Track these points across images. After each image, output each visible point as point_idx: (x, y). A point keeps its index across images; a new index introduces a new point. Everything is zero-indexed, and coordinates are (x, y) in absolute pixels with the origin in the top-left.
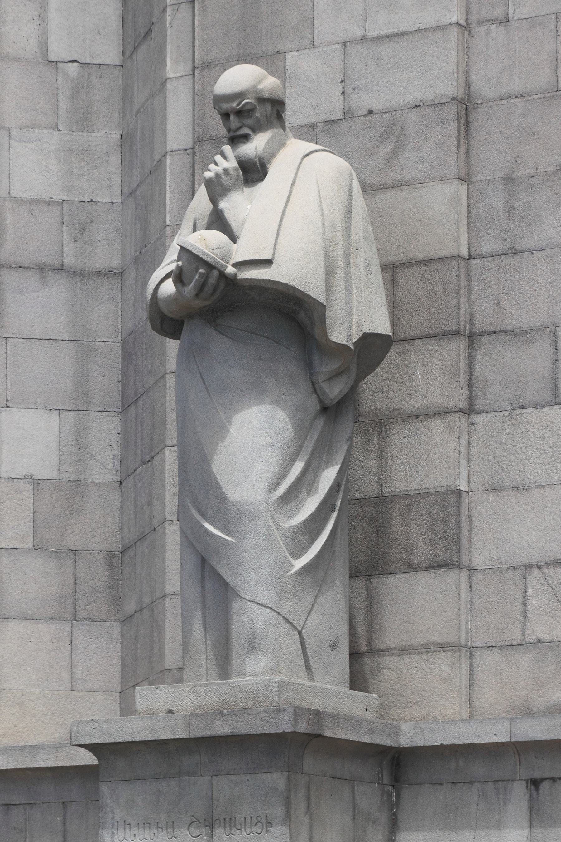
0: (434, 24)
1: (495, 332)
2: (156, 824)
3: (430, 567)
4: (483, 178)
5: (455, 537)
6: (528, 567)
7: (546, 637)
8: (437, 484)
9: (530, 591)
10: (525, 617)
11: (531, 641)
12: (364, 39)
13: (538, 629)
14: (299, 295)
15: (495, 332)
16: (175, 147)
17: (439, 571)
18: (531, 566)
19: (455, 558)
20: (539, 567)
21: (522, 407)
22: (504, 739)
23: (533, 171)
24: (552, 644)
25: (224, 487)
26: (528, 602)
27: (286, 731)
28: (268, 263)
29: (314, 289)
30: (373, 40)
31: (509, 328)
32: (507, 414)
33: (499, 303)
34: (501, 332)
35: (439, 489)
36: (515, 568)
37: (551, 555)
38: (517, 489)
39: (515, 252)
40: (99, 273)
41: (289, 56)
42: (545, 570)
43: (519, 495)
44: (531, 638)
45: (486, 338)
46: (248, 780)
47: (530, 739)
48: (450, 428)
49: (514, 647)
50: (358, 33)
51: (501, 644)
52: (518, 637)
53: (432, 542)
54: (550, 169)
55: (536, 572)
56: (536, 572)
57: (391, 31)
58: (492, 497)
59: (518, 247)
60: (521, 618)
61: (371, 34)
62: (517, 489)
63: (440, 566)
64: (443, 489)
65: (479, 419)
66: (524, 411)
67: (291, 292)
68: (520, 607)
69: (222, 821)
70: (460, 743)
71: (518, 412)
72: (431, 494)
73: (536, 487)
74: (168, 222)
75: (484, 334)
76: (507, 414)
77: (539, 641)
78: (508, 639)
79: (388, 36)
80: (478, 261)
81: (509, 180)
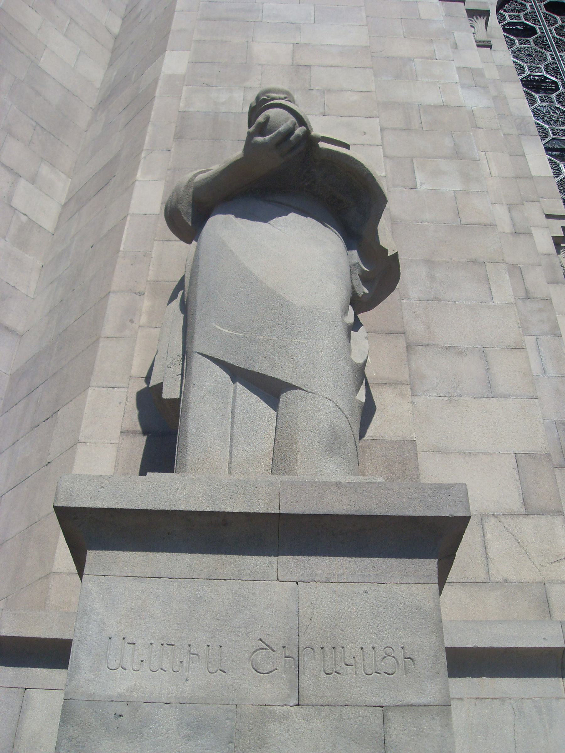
1: (428, 345)
2: (186, 646)
4: (405, 257)
5: (415, 477)
7: (513, 578)
8: (392, 434)
9: (489, 536)
10: (487, 558)
11: (498, 580)
13: (503, 569)
15: (428, 345)
18: (488, 515)
21: (460, 396)
23: (449, 260)
24: (520, 584)
26: (489, 546)
31: (441, 343)
33: (429, 328)
35: (395, 439)
38: (463, 453)
42: (503, 519)
45: (421, 347)
49: (479, 584)
51: (462, 580)
52: (482, 576)
55: (493, 520)
60: (483, 559)
62: (463, 453)
64: (398, 439)
65: (416, 399)
70: (500, 646)
71: (456, 399)
72: (386, 441)
73: (485, 454)
74: (121, 249)
76: (446, 399)
77: (506, 581)
78: (471, 577)
80: (408, 302)
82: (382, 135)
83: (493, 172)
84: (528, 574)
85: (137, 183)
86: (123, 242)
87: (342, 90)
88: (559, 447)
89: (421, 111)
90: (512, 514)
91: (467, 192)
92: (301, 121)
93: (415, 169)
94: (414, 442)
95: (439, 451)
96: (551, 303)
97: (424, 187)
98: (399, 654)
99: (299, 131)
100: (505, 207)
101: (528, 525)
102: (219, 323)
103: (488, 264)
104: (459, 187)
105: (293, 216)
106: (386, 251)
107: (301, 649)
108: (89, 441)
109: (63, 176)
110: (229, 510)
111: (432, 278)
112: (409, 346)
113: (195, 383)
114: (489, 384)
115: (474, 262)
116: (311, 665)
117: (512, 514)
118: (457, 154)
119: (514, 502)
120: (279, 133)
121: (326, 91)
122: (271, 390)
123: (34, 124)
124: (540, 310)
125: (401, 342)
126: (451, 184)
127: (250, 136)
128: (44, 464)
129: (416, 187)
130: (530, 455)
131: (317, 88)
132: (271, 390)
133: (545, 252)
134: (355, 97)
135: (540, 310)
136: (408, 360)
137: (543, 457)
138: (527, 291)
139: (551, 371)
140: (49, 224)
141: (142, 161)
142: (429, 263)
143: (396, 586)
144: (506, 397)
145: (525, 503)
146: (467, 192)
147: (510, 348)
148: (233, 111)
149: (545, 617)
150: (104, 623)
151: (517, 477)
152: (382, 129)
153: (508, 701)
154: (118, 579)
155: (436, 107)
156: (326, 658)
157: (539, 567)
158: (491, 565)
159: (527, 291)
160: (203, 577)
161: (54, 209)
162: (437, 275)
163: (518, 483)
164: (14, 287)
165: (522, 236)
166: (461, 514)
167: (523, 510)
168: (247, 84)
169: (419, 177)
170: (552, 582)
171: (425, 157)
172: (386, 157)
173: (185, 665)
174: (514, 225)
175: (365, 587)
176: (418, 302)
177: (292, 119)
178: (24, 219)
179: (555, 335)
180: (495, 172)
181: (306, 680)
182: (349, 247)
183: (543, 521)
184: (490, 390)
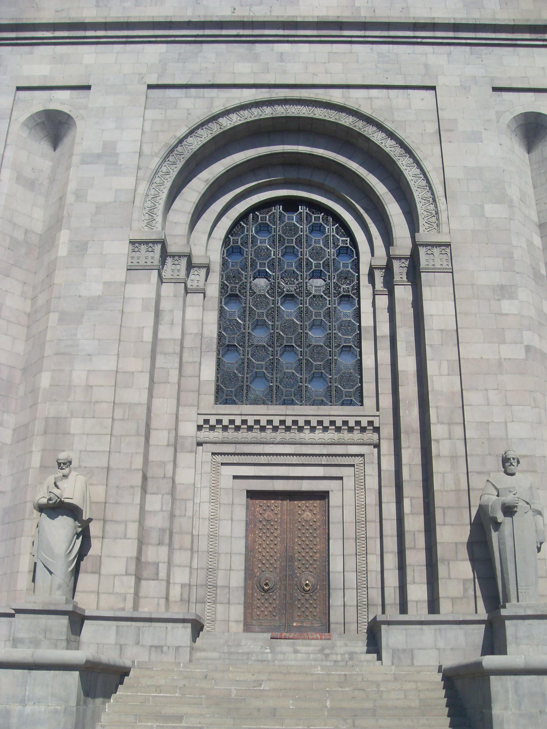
6: (115, 575)
7: (119, 592)
12: (86, 450)
13: (117, 590)
29: (80, 506)
39: (117, 503)
44: (115, 592)
50: (84, 449)
55: (117, 577)
56: (117, 577)
61: (87, 450)
75: (108, 521)
81: (117, 487)
87: (102, 402)
90: (122, 575)
92: (59, 498)
100: (168, 431)
101: (125, 578)
105: (60, 516)
109: (12, 415)
114: (125, 534)
117: (122, 575)
119: (124, 572)
121: (96, 402)
122: (51, 573)
125: (102, 522)
129: (120, 452)
131: (93, 401)
132: (51, 573)
139: (164, 509)
140: (9, 442)
144: (129, 539)
145: (126, 572)
146: (137, 453)
161: (10, 432)
168: (69, 399)
174: (168, 441)
177: (57, 498)
182: (75, 520)
183: (129, 577)
184: (125, 538)
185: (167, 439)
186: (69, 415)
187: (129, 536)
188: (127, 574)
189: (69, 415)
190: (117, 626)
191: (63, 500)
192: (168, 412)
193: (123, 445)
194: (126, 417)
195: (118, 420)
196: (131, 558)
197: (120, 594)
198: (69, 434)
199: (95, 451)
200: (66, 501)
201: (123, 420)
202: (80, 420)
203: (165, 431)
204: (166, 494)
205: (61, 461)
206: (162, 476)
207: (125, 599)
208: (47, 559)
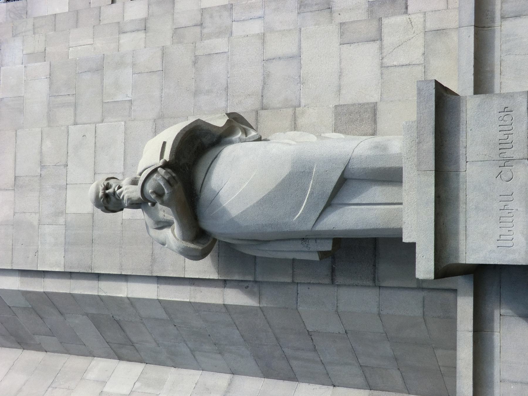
0: (123, 134)
3: (375, 122)
5: (360, 106)
6: (382, 66)
7: (422, 50)
14: (187, 129)
16: (156, 294)
17: (378, 116)
18: (382, 63)
19: (372, 105)
20: (383, 58)
22: (472, 29)
25: (283, 177)
26: (401, 64)
27: (434, 86)
28: (164, 143)
30: (124, 169)
31: (261, 88)
32: (302, 86)
34: (262, 93)
36: (382, 74)
37: (377, 51)
40: (229, 385)
41: (124, 218)
42: (384, 54)
43: (343, 74)
45: (264, 101)
46: (471, 130)
47: (474, 12)
48: (303, 113)
52: (421, 68)
53: (362, 120)
54: (194, 71)
55: (385, 60)
57: (123, 159)
58: (343, 92)
59: (225, 86)
61: (122, 170)
63: (375, 115)
65: (303, 104)
66: (301, 75)
67: (184, 132)
68: (404, 69)
69: (501, 151)
71: (302, 79)
74: (188, 300)
76: (302, 86)
79: (124, 160)
82: (81, 124)
83: (89, 43)
84: (420, 41)
85: (129, 296)
86: (182, 300)
88: (317, 12)
89: (57, 95)
90: (381, 48)
91: (134, 65)
93: (113, 100)
94: (336, 107)
95: (339, 90)
96: (205, 8)
97: (130, 95)
98: (503, 114)
99: (162, 171)
100: (122, 36)
101: (387, 40)
102: (294, 216)
103: (197, 54)
104: (129, 70)
106: (228, 120)
107: (501, 159)
108: (336, 305)
110: (433, 195)
111: (209, 92)
112: (263, 109)
113: (332, 227)
114: (292, 57)
115: (195, 63)
116: (508, 154)
117: (381, 48)
118: (99, 69)
120: (164, 185)
123: (50, 389)
124: (211, 17)
125: (262, 113)
126: (127, 75)
127: (163, 203)
128: (345, 336)
129: (130, 101)
130: (341, 35)
131: (39, 171)
133: (147, 7)
134: (48, 144)
135: (211, 17)
136: (274, 109)
137: (342, 27)
138: (196, 25)
139: (260, 13)
141: (109, 294)
142: (196, 93)
143: (468, 116)
144: (300, 48)
145: (374, 41)
146: (134, 65)
147: (264, 43)
148: (64, 231)
149: (446, 33)
150: (491, 250)
151: (356, 44)
152: (75, 124)
153: (502, 58)
154: (467, 247)
155: (51, 84)
156: (505, 147)
157: (414, 35)
158: (414, 63)
159: (196, 25)
160: (465, 207)
161: (124, 367)
162: (206, 88)
163: (360, 44)
164: (196, 384)
165: (148, 25)
166: (434, 84)
167: (378, 42)
168: (36, 223)
169: (120, 98)
170: (425, 27)
171: (102, 93)
172: (102, 121)
173: (510, 211)
174: (138, 30)
175: (469, 130)
176: (228, 101)
178: (138, 385)
179: (232, 8)
180: (90, 41)
181: (516, 156)
183: (385, 30)
184: (297, 57)
185: (134, 34)
186: (62, 220)
187: (293, 50)
188: (379, 38)
189: (62, 220)
190: (503, 18)
191: (160, 163)
192: (90, 41)
193: (119, 98)
194: (71, 99)
195: (75, 115)
196: (342, 34)
197: (426, 45)
198: (93, 215)
199: (125, 152)
200: (167, 157)
201: (76, 106)
202: (70, 193)
203: (121, 41)
204: (231, 15)
205: (101, 194)
206: (198, 29)
207: (440, 32)
208: (312, 193)
